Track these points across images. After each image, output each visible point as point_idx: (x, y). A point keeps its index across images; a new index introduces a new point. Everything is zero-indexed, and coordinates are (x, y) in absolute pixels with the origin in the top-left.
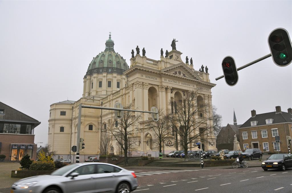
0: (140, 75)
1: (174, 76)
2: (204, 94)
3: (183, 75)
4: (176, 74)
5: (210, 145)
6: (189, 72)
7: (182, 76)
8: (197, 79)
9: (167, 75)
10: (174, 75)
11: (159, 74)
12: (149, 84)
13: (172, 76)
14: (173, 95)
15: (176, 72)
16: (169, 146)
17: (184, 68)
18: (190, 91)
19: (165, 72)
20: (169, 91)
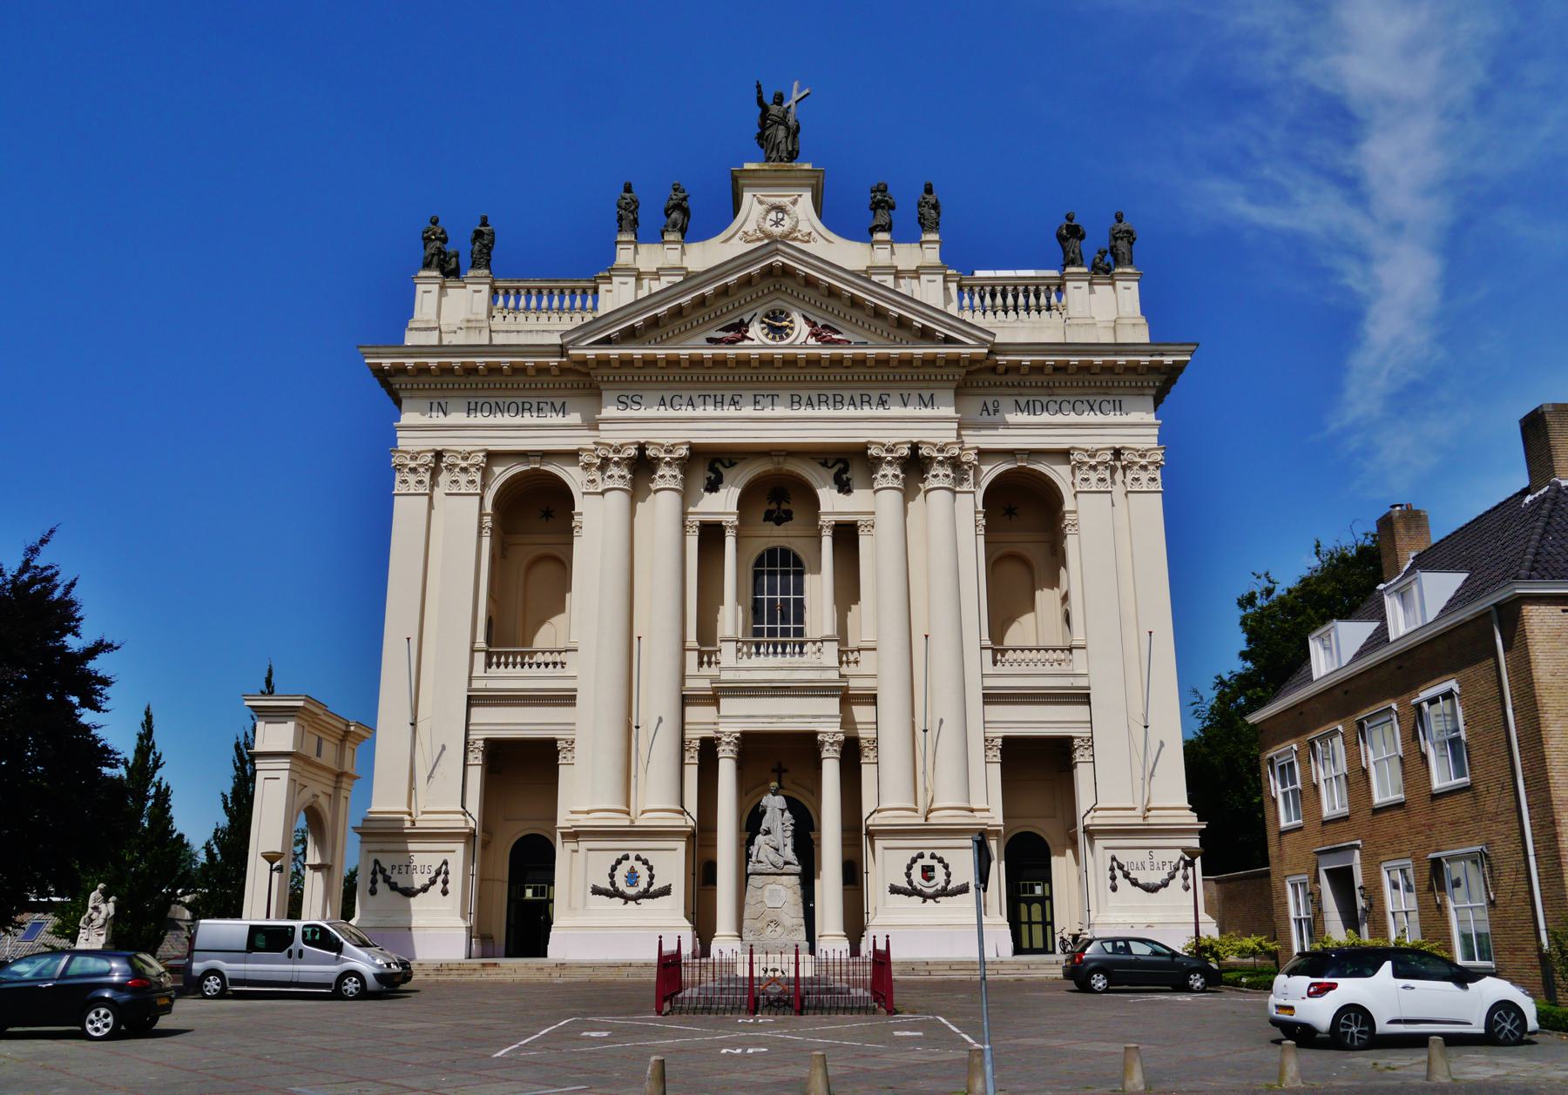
0: (429, 401)
1: (720, 362)
2: (1064, 455)
3: (813, 334)
4: (744, 338)
5: (1121, 881)
6: (855, 302)
7: (804, 345)
8: (948, 340)
9: (649, 362)
10: (730, 352)
11: (562, 369)
12: (492, 456)
13: (697, 362)
14: (722, 504)
15: (740, 328)
16: (627, 898)
17: (809, 282)
18: (873, 451)
19: (607, 341)
20: (667, 477)
